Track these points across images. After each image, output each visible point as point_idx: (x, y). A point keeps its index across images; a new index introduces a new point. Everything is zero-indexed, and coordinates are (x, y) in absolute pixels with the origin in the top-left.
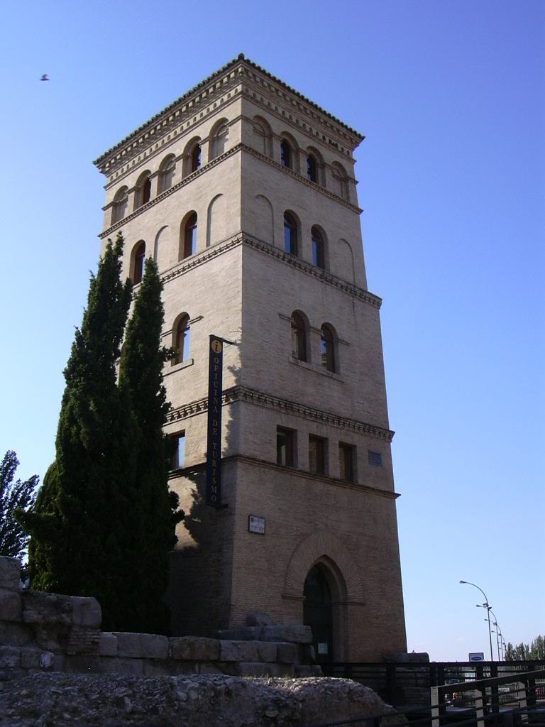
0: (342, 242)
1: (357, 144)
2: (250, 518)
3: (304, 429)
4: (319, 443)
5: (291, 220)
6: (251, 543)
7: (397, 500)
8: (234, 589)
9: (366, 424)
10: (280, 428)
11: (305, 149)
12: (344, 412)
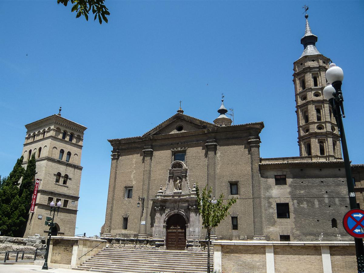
1: (85, 130)
2: (39, 215)
5: (62, 151)
7: (77, 212)
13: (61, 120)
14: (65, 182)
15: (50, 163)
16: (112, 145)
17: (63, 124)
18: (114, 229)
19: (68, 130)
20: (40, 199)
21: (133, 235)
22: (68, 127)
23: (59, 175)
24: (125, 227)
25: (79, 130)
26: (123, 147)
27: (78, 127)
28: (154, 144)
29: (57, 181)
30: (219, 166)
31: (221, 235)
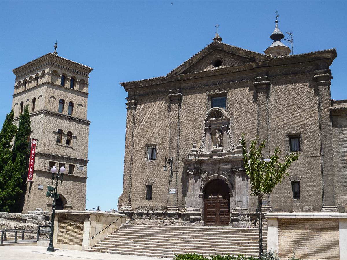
1: (90, 71)
2: (39, 185)
5: (62, 102)
7: (87, 179)
13: (57, 60)
14: (68, 142)
15: (48, 118)
16: (126, 90)
17: (60, 66)
18: (134, 200)
19: (67, 73)
20: (39, 164)
21: (160, 208)
22: (67, 69)
23: (60, 132)
24: (150, 198)
25: (81, 73)
26: (142, 92)
27: (81, 68)
28: (182, 86)
29: (59, 140)
30: (274, 112)
31: (278, 206)
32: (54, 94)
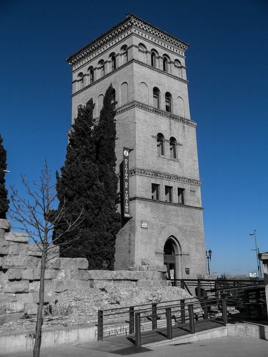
0: (179, 98)
3: (163, 183)
4: (168, 189)
5: (156, 91)
6: (142, 232)
8: (136, 251)
9: (189, 180)
10: (153, 184)
11: (162, 56)
12: (180, 175)
23: (160, 136)
32: (145, 79)
